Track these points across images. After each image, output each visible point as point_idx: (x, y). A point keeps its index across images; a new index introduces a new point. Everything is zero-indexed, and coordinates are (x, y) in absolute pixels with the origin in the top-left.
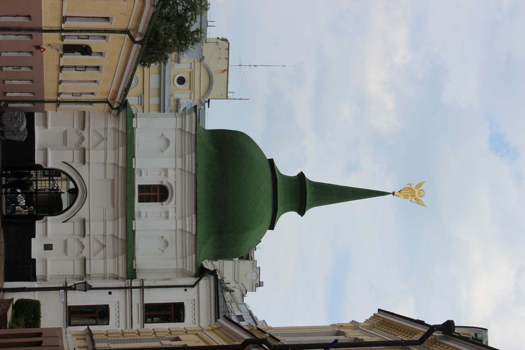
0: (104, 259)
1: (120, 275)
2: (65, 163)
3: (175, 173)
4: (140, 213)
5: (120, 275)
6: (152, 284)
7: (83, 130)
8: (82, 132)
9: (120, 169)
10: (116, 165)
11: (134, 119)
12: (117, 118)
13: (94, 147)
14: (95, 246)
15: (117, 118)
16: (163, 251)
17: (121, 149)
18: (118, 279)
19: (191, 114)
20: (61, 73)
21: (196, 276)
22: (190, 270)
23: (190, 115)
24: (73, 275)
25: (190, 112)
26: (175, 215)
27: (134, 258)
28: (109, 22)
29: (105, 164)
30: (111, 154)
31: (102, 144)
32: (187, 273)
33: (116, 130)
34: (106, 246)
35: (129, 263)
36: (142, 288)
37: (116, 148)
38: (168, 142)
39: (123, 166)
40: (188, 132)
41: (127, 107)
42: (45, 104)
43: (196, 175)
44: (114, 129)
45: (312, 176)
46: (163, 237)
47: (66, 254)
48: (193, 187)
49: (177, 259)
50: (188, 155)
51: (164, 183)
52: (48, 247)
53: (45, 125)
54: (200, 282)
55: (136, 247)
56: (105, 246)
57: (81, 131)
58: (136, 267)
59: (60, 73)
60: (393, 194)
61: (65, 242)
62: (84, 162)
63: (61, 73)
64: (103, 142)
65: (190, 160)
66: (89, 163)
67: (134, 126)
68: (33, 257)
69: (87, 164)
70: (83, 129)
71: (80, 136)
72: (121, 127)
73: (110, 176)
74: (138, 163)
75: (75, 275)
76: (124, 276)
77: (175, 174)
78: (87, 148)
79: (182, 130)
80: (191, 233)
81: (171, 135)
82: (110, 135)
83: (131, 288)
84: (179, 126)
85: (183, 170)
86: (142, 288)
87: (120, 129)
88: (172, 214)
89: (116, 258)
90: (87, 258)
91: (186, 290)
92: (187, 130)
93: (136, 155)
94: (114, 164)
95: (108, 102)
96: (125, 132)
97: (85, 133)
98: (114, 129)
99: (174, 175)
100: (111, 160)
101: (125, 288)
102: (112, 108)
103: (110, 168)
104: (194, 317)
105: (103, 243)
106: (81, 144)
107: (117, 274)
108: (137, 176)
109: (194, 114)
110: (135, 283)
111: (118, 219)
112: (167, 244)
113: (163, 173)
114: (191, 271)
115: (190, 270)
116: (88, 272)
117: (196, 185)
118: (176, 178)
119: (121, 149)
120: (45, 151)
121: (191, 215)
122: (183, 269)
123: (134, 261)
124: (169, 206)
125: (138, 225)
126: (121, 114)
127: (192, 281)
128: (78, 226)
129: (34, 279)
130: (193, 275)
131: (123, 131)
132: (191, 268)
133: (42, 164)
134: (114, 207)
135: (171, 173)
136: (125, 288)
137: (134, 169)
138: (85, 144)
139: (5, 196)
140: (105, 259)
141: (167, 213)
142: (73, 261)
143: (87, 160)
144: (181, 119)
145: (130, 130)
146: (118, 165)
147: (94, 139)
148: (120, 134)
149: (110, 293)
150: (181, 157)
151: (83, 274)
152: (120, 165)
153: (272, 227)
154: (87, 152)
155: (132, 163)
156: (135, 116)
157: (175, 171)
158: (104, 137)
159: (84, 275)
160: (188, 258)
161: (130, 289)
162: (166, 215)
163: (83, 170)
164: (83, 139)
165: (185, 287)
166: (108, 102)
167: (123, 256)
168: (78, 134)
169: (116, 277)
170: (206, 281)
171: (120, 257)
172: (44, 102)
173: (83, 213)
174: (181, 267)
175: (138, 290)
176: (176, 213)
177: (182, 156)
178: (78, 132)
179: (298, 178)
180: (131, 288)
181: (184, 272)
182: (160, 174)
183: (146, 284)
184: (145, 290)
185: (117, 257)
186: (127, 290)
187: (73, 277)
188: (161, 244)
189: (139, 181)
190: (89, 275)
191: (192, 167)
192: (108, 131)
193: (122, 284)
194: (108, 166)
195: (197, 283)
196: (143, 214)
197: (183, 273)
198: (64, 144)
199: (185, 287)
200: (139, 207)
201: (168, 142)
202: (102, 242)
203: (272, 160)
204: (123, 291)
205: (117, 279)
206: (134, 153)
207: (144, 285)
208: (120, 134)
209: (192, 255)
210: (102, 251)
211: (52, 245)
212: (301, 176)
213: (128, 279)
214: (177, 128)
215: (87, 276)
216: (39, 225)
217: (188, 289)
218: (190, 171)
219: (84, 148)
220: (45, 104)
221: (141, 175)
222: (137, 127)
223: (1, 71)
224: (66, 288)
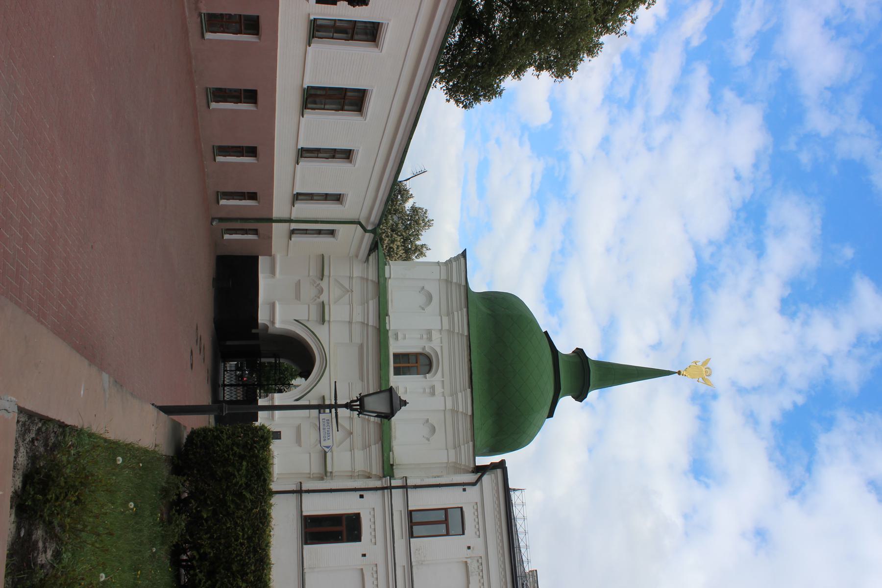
0: (351, 451)
1: (374, 472)
3: (441, 336)
5: (374, 472)
6: (418, 482)
7: (322, 280)
8: (320, 282)
9: (370, 329)
10: (364, 324)
11: (387, 267)
12: (366, 264)
13: (335, 303)
15: (366, 264)
16: (428, 440)
17: (371, 302)
18: (371, 478)
19: (458, 260)
20: (303, 117)
22: (466, 463)
23: (457, 262)
24: (310, 474)
25: (457, 258)
26: (443, 390)
27: (390, 449)
28: (362, 116)
30: (358, 310)
32: (463, 467)
34: (354, 433)
35: (386, 455)
36: (405, 487)
37: (364, 302)
38: (430, 298)
39: (374, 325)
40: (456, 283)
41: (378, 249)
42: (273, 224)
43: (469, 336)
44: (362, 278)
46: (427, 421)
47: (300, 445)
48: (466, 353)
49: (447, 449)
50: (456, 313)
51: (428, 350)
53: (273, 272)
54: (483, 478)
55: (393, 434)
56: (352, 433)
57: (318, 282)
58: (393, 462)
59: (301, 117)
60: (679, 373)
62: (323, 321)
63: (303, 117)
64: (348, 295)
66: (329, 321)
67: (387, 275)
69: (326, 324)
70: (321, 277)
71: (318, 288)
72: (372, 275)
73: (357, 339)
74: (394, 323)
75: (312, 473)
76: (380, 473)
77: (441, 338)
78: (326, 303)
80: (464, 413)
82: (357, 286)
83: (391, 488)
84: (444, 277)
85: (451, 332)
87: (370, 278)
88: (439, 390)
89: (368, 449)
92: (455, 280)
93: (390, 313)
94: (363, 323)
95: (359, 223)
96: (377, 281)
97: (324, 284)
98: (362, 278)
99: (439, 339)
100: (358, 317)
101: (383, 488)
102: (365, 230)
103: (357, 329)
104: (477, 526)
105: (348, 428)
106: (319, 298)
107: (369, 471)
108: (392, 341)
109: (462, 260)
112: (433, 430)
113: (425, 336)
114: (467, 464)
115: (466, 463)
116: (329, 469)
117: (469, 351)
118: (441, 343)
119: (371, 302)
120: (273, 306)
121: (465, 390)
122: (455, 463)
123: (391, 453)
124: (435, 379)
126: (371, 258)
130: (470, 470)
131: (374, 280)
133: (268, 324)
134: (362, 380)
135: (436, 336)
136: (383, 488)
137: (388, 331)
138: (324, 297)
139: (222, 388)
140: (352, 451)
142: (308, 455)
143: (327, 318)
144: (445, 267)
145: (382, 278)
146: (367, 325)
147: (335, 292)
148: (370, 283)
149: (362, 496)
150: (448, 315)
151: (322, 472)
152: (371, 323)
153: (551, 415)
155: (386, 323)
156: (387, 264)
157: (441, 334)
158: (348, 288)
159: (324, 474)
160: (462, 447)
161: (389, 490)
162: (432, 391)
163: (322, 332)
164: (321, 291)
166: (359, 223)
167: (377, 445)
168: (315, 285)
169: (368, 475)
170: (491, 477)
171: (373, 447)
172: (271, 220)
174: (454, 460)
175: (400, 490)
176: (443, 388)
177: (450, 314)
178: (315, 282)
179: (574, 354)
180: (391, 488)
181: (458, 466)
182: (422, 338)
183: (410, 483)
185: (369, 447)
186: (386, 491)
187: (308, 476)
189: (395, 347)
190: (331, 472)
191: (463, 326)
192: (354, 280)
193: (378, 484)
194: (354, 326)
195: (479, 479)
197: (457, 469)
198: (296, 298)
201: (430, 298)
202: (348, 428)
203: (546, 331)
204: (379, 492)
205: (369, 477)
206: (387, 311)
207: (408, 484)
208: (370, 283)
209: (468, 443)
210: (349, 439)
211: (280, 432)
213: (384, 476)
214: (442, 278)
215: (328, 474)
217: (467, 487)
218: (461, 332)
219: (323, 302)
220: (274, 224)
221: (397, 339)
222: (390, 278)
223: (218, 205)
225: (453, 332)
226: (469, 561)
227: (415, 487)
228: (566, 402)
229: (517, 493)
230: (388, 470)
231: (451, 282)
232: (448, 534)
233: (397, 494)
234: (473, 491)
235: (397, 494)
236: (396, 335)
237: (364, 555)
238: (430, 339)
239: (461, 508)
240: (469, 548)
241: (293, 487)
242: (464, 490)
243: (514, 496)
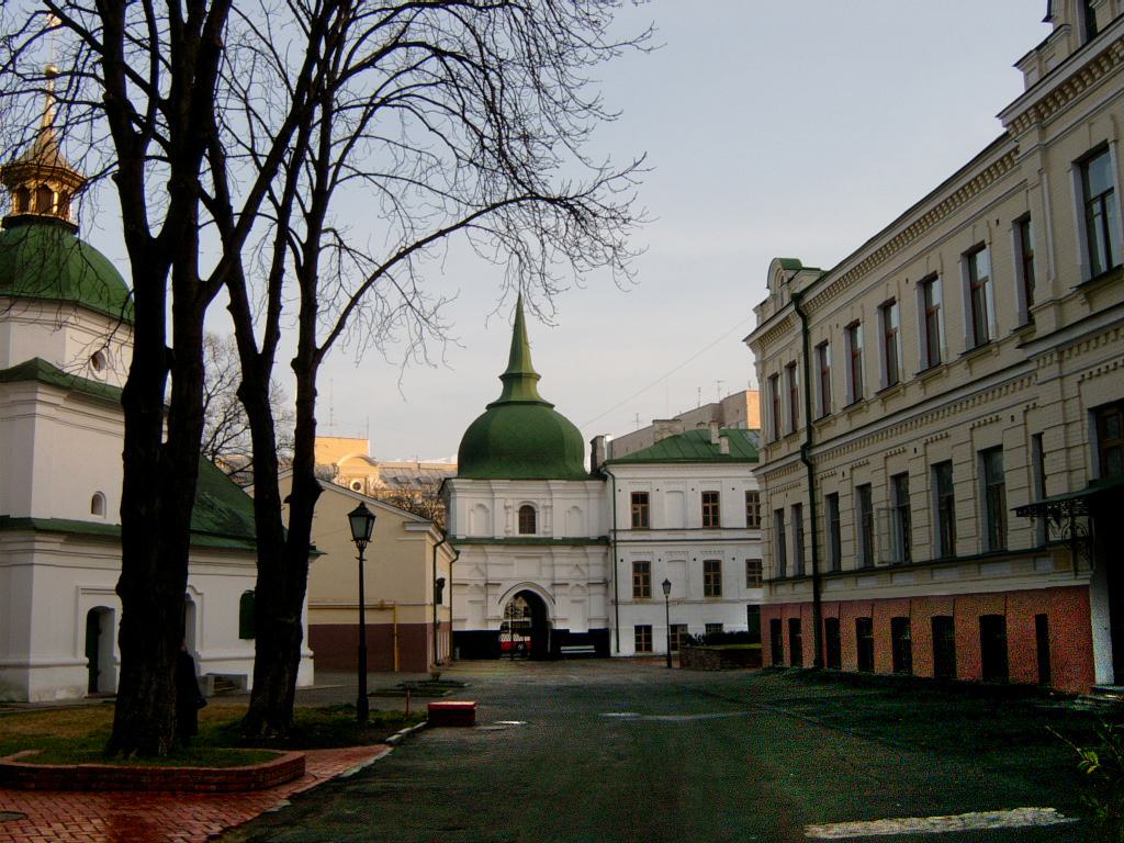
21: (604, 478)
45: (503, 367)
51: (518, 508)
53: (465, 620)
74: (500, 534)
86: (615, 531)
97: (472, 584)
108: (511, 535)
116: (601, 581)
120: (487, 621)
125: (558, 534)
127: (610, 481)
128: (558, 590)
132: (594, 485)
153: (552, 406)
163: (506, 585)
164: (477, 585)
173: (545, 585)
184: (617, 528)
189: (517, 534)
200: (541, 531)
212: (502, 378)
216: (559, 626)
224: (616, 603)
230: (603, 541)
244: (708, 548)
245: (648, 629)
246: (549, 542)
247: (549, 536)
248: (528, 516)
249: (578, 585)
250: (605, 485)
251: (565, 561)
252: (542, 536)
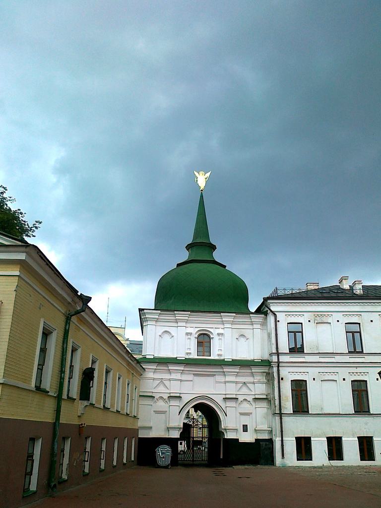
2: (179, 413)
4: (219, 355)
6: (274, 346)
11: (147, 357)
14: (244, 390)
16: (247, 339)
21: (266, 314)
27: (253, 361)
29: (181, 381)
31: (167, 383)
33: (155, 371)
35: (257, 364)
37: (169, 372)
38: (166, 332)
52: (245, 429)
61: (241, 414)
64: (164, 381)
65: (180, 315)
66: (180, 393)
68: (253, 441)
73: (191, 377)
74: (181, 355)
79: (157, 320)
81: (160, 330)
83: (279, 362)
84: (154, 323)
85: (187, 321)
86: (278, 354)
88: (221, 331)
90: (254, 397)
91: (279, 321)
97: (157, 396)
100: (178, 376)
101: (278, 366)
108: (191, 357)
110: (275, 359)
111: (224, 372)
112: (242, 335)
116: (265, 397)
120: (168, 429)
125: (228, 357)
127: (271, 318)
128: (229, 404)
129: (270, 441)
135: (189, 330)
136: (278, 366)
141: (219, 334)
143: (178, 395)
147: (161, 389)
149: (282, 379)
153: (225, 267)
154: (172, 395)
160: (252, 320)
163: (186, 398)
165: (276, 321)
173: (219, 399)
180: (279, 362)
182: (190, 339)
183: (274, 351)
186: (280, 365)
188: (242, 339)
189: (194, 355)
193: (275, 369)
196: (220, 353)
197: (264, 324)
199: (276, 321)
216: (229, 436)
224: (281, 415)
225: (187, 320)
226: (316, 322)
227: (277, 348)
228: (217, 256)
229: (279, 292)
230: (266, 363)
231: (158, 319)
232: (302, 332)
233: (282, 359)
234: (280, 316)
235: (283, 358)
236: (187, 354)
237: (314, 379)
238: (191, 334)
239: (288, 323)
240: (309, 321)
241: (278, 418)
242: (279, 321)
243: (280, 293)
244: (354, 370)
245: (307, 440)
246: (221, 363)
247: (222, 358)
248: (204, 340)
249: (245, 400)
250: (266, 319)
251: (233, 379)
252: (217, 358)
